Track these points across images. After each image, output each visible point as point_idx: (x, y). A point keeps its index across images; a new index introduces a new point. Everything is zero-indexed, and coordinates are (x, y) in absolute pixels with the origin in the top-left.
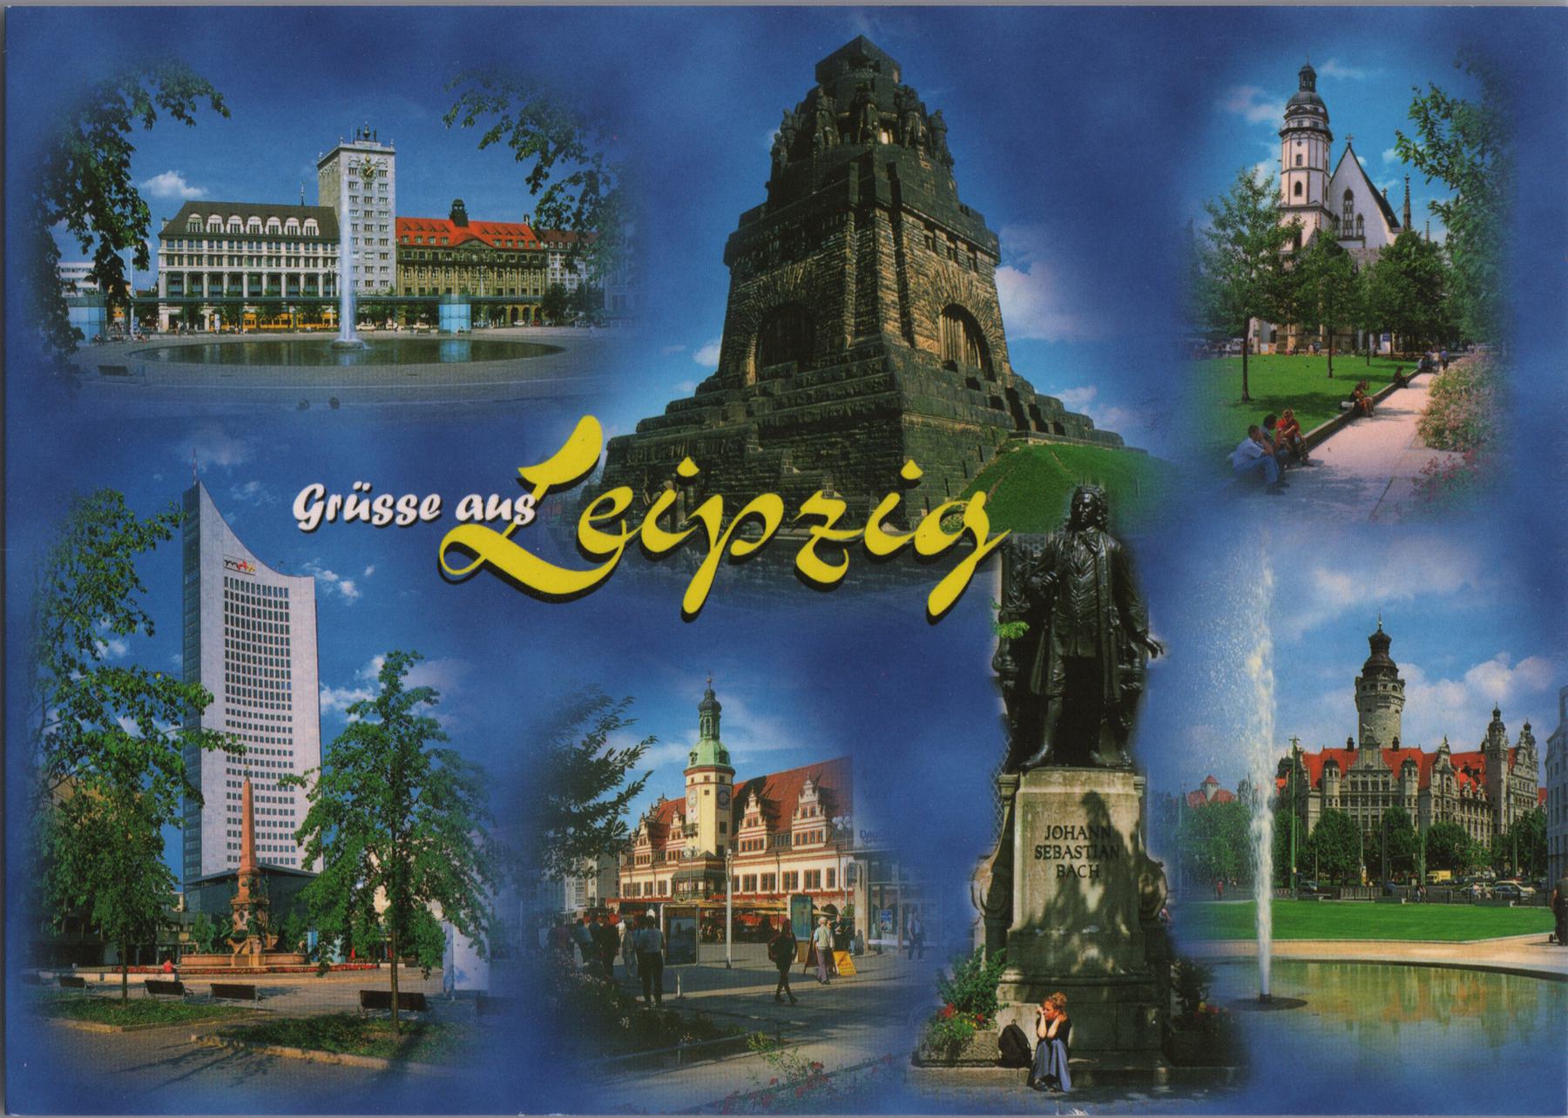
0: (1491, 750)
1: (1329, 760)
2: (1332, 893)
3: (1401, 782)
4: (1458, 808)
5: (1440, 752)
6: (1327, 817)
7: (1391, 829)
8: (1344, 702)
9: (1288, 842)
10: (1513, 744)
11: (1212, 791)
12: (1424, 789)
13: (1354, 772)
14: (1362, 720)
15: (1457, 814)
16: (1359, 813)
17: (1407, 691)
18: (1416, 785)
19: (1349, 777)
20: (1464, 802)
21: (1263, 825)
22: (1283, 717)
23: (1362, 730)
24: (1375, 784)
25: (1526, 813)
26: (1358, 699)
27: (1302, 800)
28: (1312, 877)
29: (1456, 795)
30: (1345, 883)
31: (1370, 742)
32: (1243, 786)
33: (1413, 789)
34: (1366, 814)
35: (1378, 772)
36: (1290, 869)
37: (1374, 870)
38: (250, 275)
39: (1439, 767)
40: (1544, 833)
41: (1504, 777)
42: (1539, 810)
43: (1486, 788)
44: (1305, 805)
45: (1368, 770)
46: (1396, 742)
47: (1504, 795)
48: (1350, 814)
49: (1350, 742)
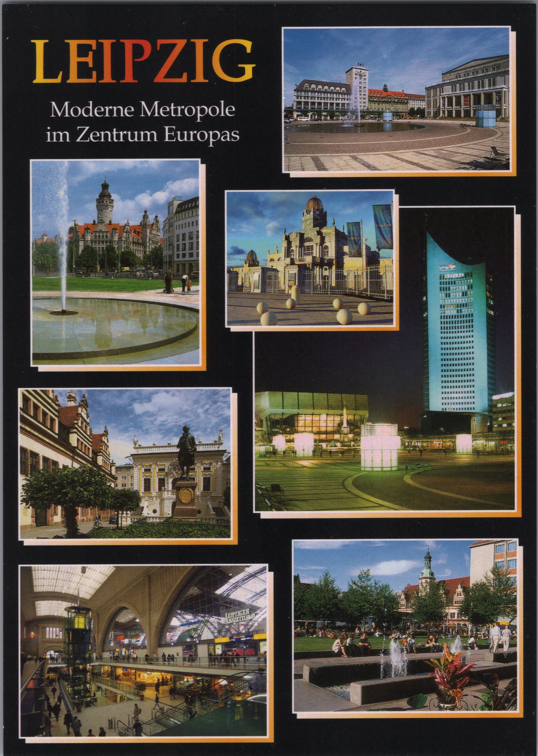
0: (144, 225)
1: (87, 228)
2: (87, 274)
3: (112, 236)
4: (132, 244)
5: (126, 225)
6: (86, 248)
7: (108, 252)
8: (92, 207)
9: (72, 257)
10: (151, 223)
11: (45, 238)
12: (120, 238)
13: (96, 232)
14: (99, 214)
15: (132, 246)
16: (97, 246)
17: (114, 204)
18: (117, 237)
19: (94, 234)
20: (134, 243)
21: (63, 250)
22: (71, 212)
23: (98, 217)
24: (103, 236)
25: (156, 247)
26: (98, 207)
27: (77, 241)
28: (80, 269)
29: (131, 240)
30: (92, 271)
31: (101, 222)
32: (57, 237)
33: (116, 238)
34: (100, 247)
35: (104, 232)
36: (72, 266)
37: (102, 267)
38: (324, 103)
39: (125, 230)
40: (162, 254)
41: (148, 234)
42: (160, 246)
43: (142, 238)
44: (78, 243)
45: (101, 231)
46: (110, 222)
47: (148, 240)
48: (94, 246)
49: (94, 222)
